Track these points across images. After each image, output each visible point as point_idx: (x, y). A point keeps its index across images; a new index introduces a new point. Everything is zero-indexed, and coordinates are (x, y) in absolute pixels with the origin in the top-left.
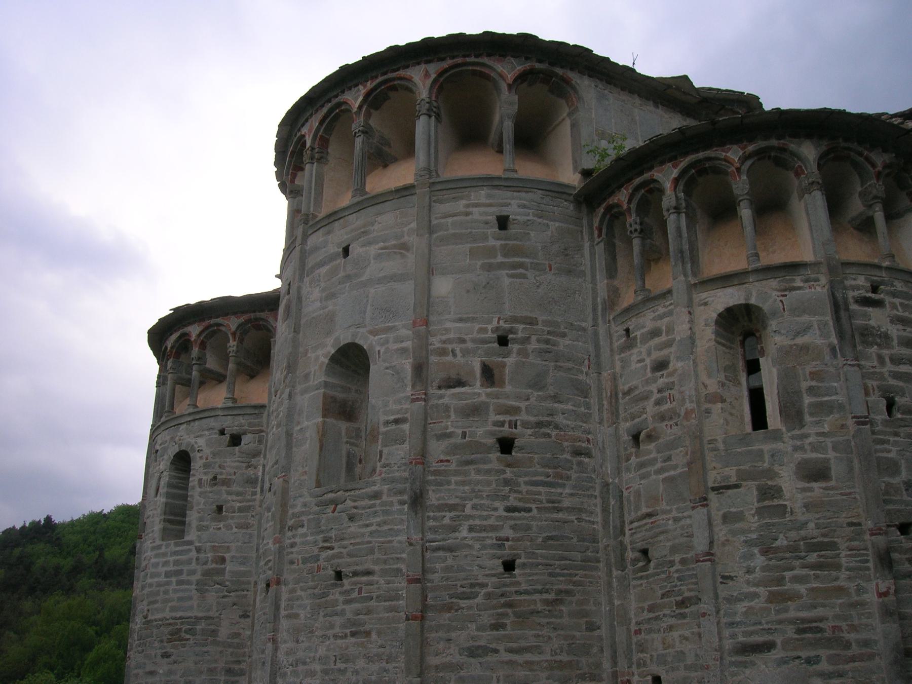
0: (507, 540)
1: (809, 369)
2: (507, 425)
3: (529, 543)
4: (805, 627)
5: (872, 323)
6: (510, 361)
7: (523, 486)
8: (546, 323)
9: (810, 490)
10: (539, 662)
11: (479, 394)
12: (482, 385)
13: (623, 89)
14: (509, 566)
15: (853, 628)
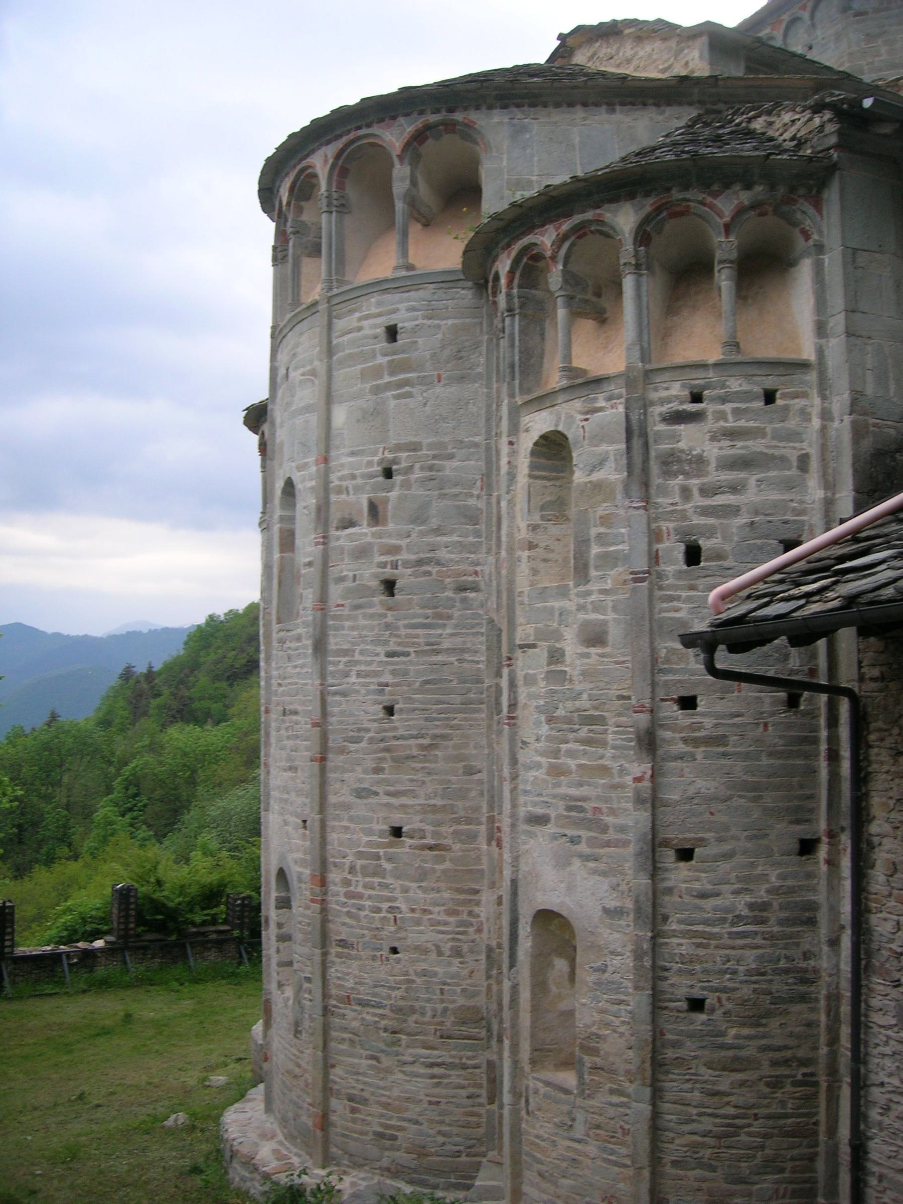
0: (387, 685)
1: (600, 512)
2: (389, 566)
3: (406, 688)
4: (574, 805)
5: (682, 445)
6: (394, 494)
7: (402, 630)
8: (431, 446)
9: (587, 656)
10: (413, 806)
11: (366, 534)
12: (369, 525)
13: (557, 105)
14: (390, 710)
15: (613, 812)
